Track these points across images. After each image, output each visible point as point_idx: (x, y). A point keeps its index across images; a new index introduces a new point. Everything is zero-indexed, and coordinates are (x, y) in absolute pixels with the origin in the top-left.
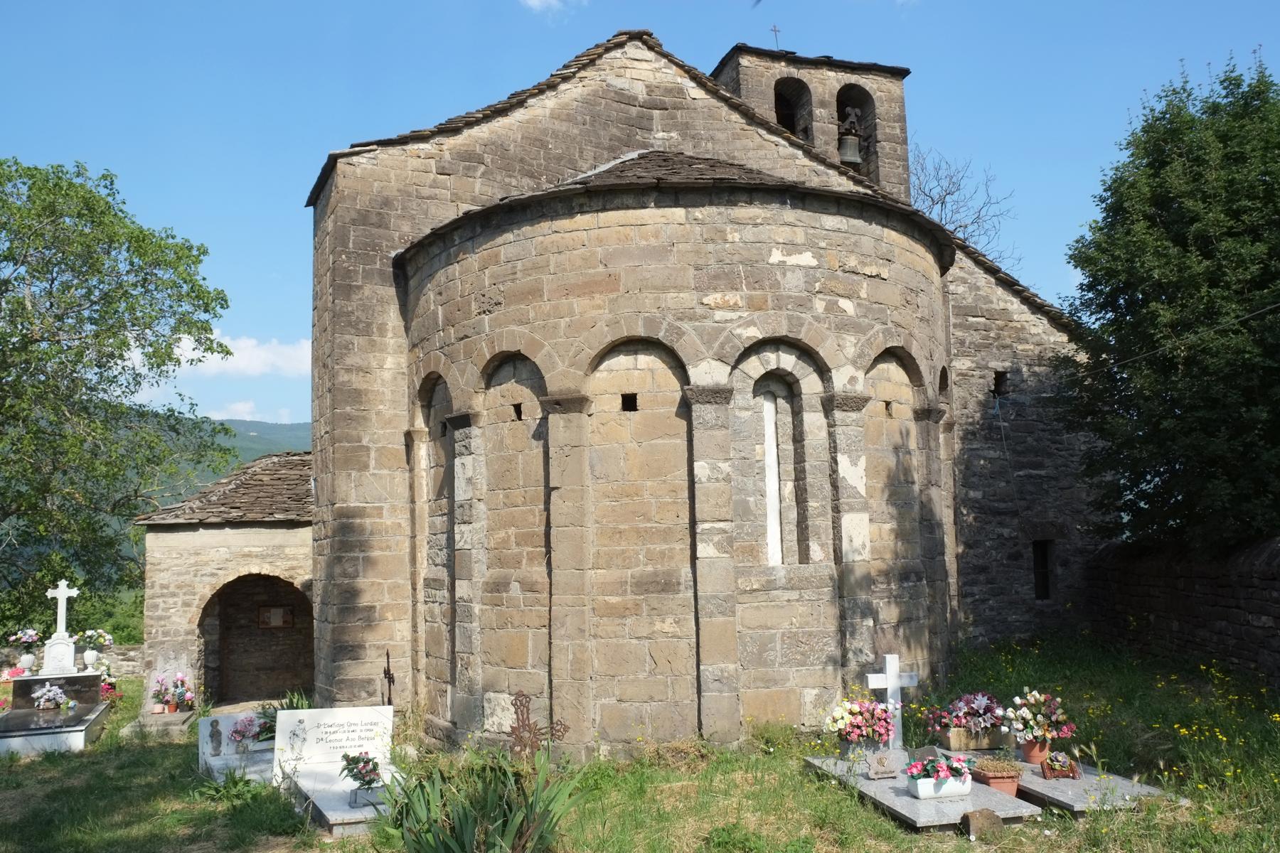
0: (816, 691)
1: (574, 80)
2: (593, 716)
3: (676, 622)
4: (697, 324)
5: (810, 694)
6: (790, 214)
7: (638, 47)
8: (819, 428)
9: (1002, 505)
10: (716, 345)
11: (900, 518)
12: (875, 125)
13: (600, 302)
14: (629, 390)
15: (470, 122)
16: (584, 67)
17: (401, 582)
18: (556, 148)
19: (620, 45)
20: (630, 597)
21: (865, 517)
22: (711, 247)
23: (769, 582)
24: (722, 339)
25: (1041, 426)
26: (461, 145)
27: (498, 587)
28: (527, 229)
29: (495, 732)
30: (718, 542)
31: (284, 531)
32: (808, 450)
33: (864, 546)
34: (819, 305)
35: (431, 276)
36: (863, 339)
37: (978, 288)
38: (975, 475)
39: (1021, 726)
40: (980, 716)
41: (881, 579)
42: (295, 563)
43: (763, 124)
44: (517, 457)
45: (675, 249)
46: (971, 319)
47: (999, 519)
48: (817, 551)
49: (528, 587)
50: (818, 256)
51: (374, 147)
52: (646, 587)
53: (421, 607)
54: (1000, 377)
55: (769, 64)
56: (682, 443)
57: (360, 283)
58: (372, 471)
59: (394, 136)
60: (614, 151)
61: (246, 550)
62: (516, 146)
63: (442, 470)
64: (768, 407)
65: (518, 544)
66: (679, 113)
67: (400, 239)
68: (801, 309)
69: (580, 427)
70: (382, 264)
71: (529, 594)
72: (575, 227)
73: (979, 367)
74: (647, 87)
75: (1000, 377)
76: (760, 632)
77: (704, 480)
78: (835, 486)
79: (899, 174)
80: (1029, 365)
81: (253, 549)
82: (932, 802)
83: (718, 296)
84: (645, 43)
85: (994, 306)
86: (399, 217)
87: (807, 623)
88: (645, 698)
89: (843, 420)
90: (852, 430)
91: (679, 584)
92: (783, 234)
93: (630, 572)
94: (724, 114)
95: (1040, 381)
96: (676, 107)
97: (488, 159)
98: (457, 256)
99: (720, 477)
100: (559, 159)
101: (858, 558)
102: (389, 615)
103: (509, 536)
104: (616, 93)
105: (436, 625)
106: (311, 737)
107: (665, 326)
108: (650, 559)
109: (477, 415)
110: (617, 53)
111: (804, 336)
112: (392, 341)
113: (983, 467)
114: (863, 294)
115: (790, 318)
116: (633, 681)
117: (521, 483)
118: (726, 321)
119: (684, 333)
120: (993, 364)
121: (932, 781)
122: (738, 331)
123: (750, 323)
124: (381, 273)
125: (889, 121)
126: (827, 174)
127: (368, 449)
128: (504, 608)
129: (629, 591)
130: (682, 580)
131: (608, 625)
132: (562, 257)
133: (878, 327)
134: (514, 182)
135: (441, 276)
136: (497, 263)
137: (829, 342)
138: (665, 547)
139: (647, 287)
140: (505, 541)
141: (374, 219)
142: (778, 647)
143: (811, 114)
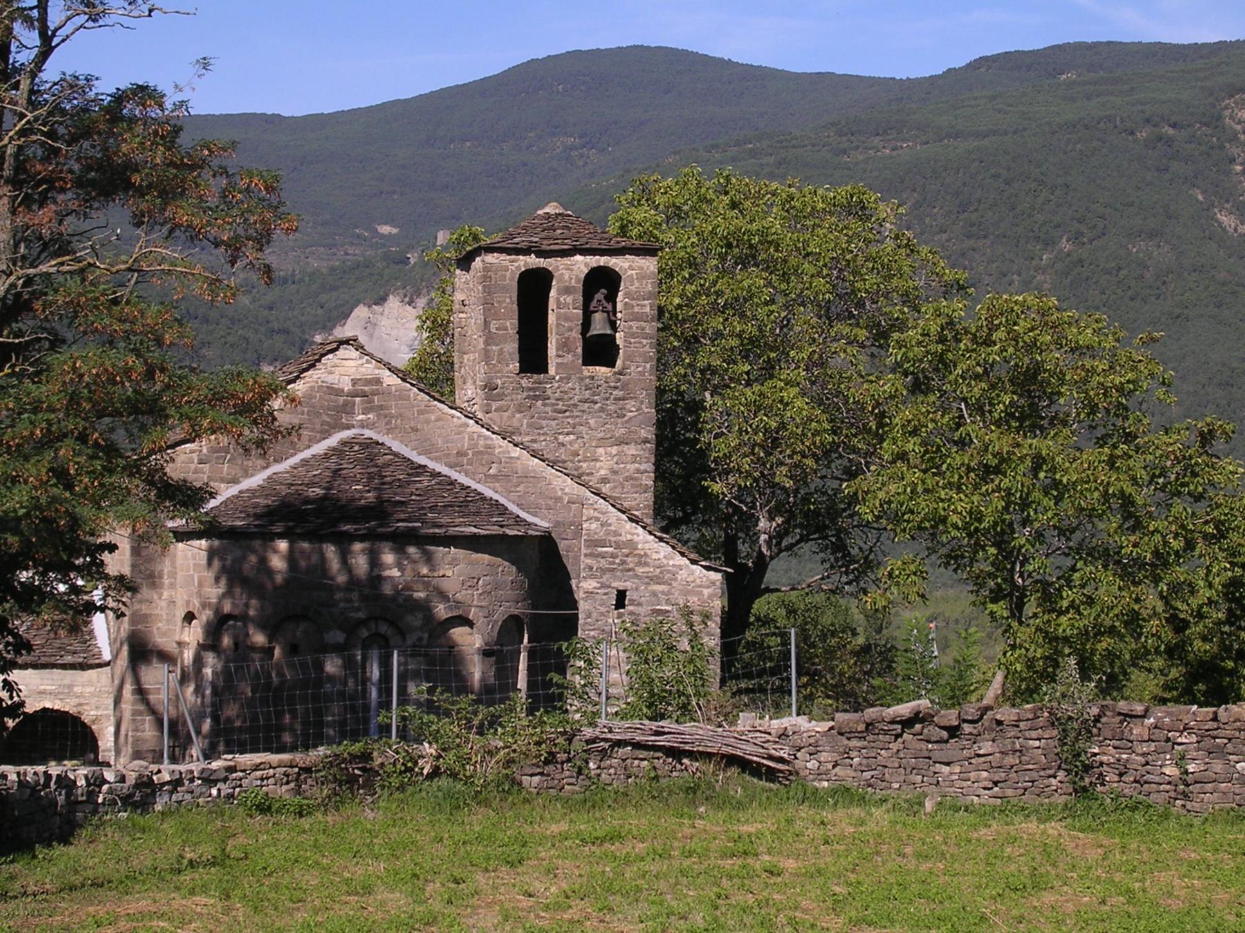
42: (82, 701)
46: (599, 549)
60: (326, 434)
61: (42, 687)
81: (50, 687)
120: (615, 584)
122: (352, 614)
125: (638, 299)
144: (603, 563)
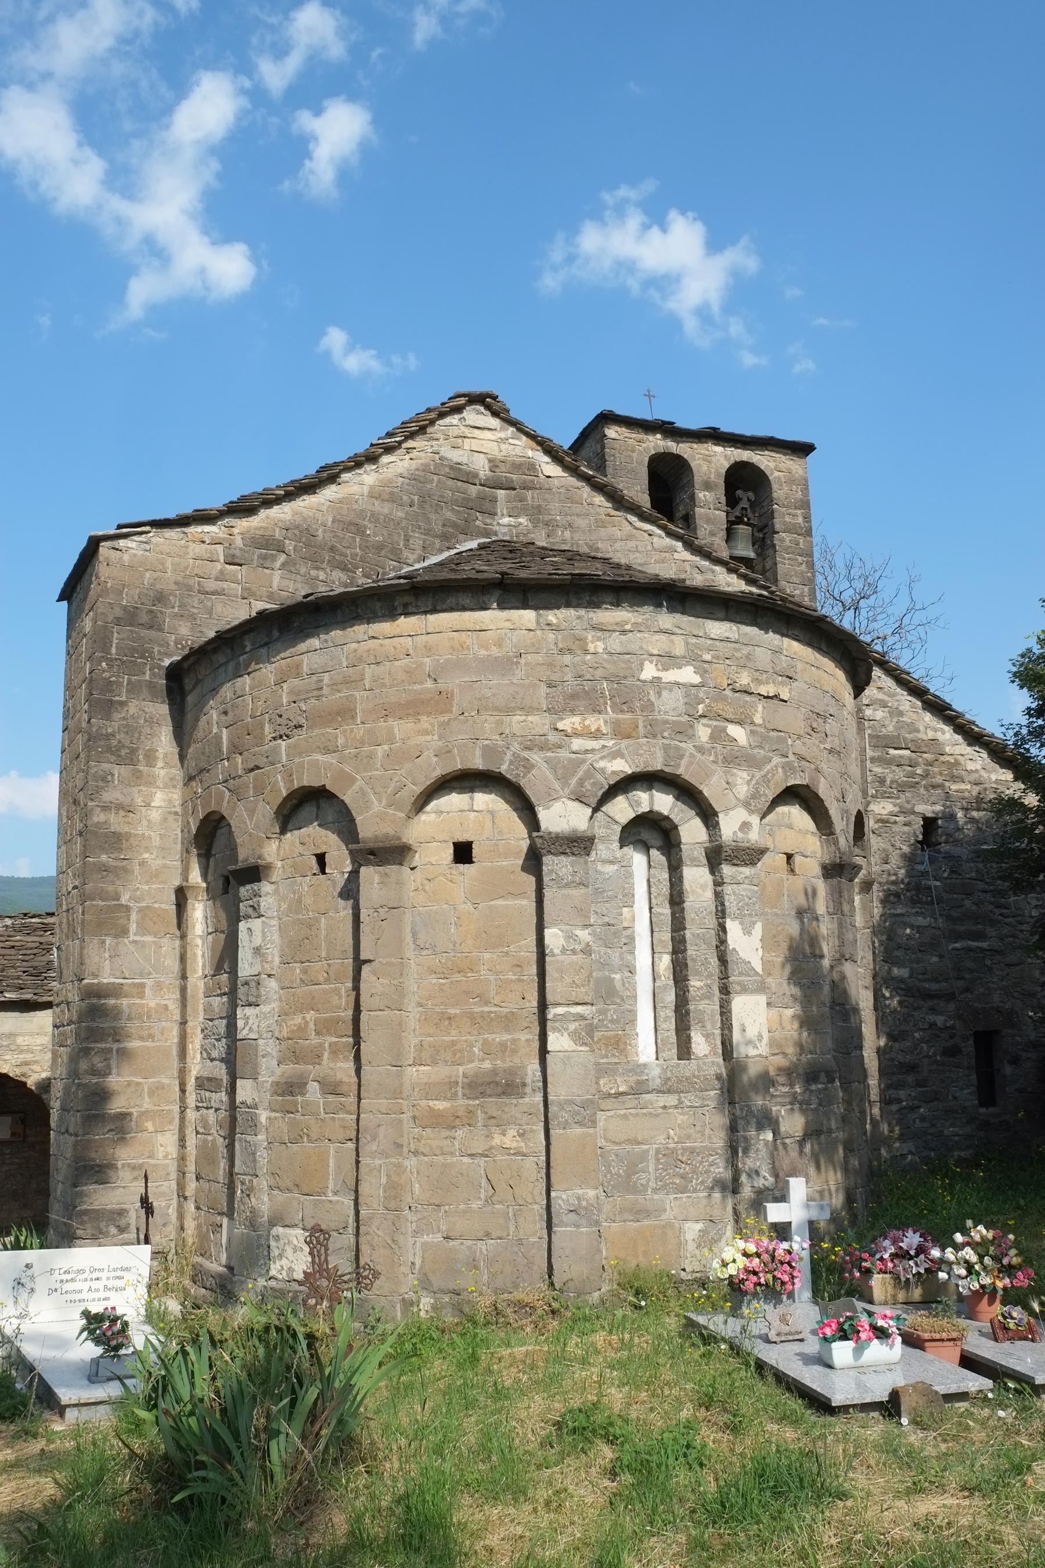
0: (699, 1226)
1: (399, 452)
2: (411, 1259)
3: (521, 1135)
4: (549, 754)
5: (693, 1230)
6: (666, 619)
7: (479, 413)
8: (703, 887)
9: (934, 986)
10: (574, 781)
11: (806, 1001)
12: (773, 512)
13: (426, 726)
14: (462, 838)
15: (269, 500)
16: (412, 436)
17: (166, 1081)
18: (375, 535)
19: (458, 410)
20: (461, 1102)
21: (762, 999)
22: (567, 659)
23: (639, 1083)
24: (580, 773)
25: (982, 886)
26: (257, 528)
27: (291, 1088)
28: (336, 634)
29: (284, 1280)
30: (575, 1032)
31: (16, 1014)
32: (690, 915)
33: (760, 1037)
34: (703, 732)
35: (215, 690)
36: (758, 775)
37: (901, 714)
38: (899, 947)
39: (963, 1272)
40: (911, 1258)
41: (782, 1079)
42: (29, 1057)
43: (633, 509)
44: (318, 921)
45: (523, 661)
46: (892, 751)
47: (930, 1003)
48: (700, 1044)
49: (331, 1088)
50: (701, 672)
51: (148, 528)
52: (481, 1089)
53: (191, 1115)
54: (929, 823)
55: (642, 436)
56: (529, 904)
57: (124, 698)
58: (132, 938)
59: (172, 515)
60: (447, 539)
62: (325, 531)
63: (223, 936)
64: (638, 860)
65: (318, 1033)
66: (529, 494)
67: (176, 643)
68: (679, 737)
69: (400, 883)
70: (153, 675)
71: (331, 1098)
72: (398, 632)
73: (903, 812)
74: (490, 461)
75: (929, 823)
76: (628, 1147)
77: (557, 951)
78: (723, 960)
79: (802, 572)
80: (966, 810)
82: (852, 1373)
83: (577, 719)
84: (488, 407)
85: (921, 736)
86: (175, 616)
87: (689, 1137)
88: (480, 1235)
89: (733, 877)
90: (744, 890)
91: (524, 1085)
92: (657, 644)
93: (461, 1069)
94: (585, 496)
95: (979, 829)
96: (525, 487)
97: (289, 545)
98: (248, 666)
99: (578, 947)
100: (379, 547)
101: (752, 1052)
102: (149, 1126)
103: (307, 1023)
104: (451, 468)
105: (210, 1138)
106: (42, 1285)
107: (509, 756)
108: (487, 1052)
109: (268, 867)
110: (453, 419)
111: (683, 770)
112: (162, 772)
113: (910, 937)
114: (758, 719)
115: (666, 748)
116: (464, 1212)
117: (324, 954)
118: (587, 751)
119: (533, 766)
121: (850, 1344)
122: (601, 764)
123: (617, 754)
124: (151, 686)
125: (788, 507)
126: (713, 572)
127: (128, 909)
128: (298, 1116)
129: (460, 1094)
130: (528, 1080)
131: (433, 1138)
132: (381, 669)
133: (777, 760)
134: (322, 576)
135: (227, 691)
136: (298, 675)
137: (714, 779)
138: (506, 1037)
139: (487, 709)
140: (302, 1029)
141: (144, 618)
142: (651, 1168)
143: (692, 497)
144: (900, 774)
